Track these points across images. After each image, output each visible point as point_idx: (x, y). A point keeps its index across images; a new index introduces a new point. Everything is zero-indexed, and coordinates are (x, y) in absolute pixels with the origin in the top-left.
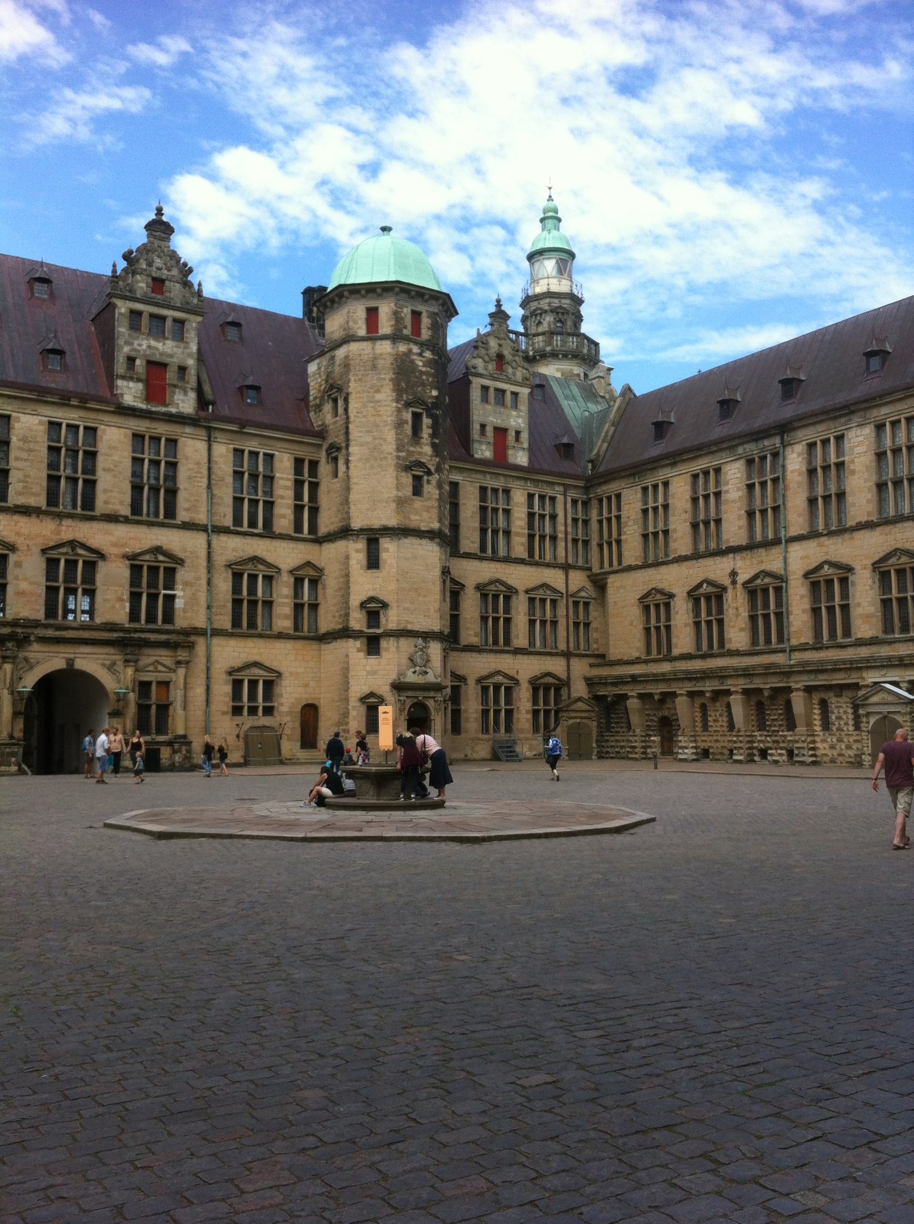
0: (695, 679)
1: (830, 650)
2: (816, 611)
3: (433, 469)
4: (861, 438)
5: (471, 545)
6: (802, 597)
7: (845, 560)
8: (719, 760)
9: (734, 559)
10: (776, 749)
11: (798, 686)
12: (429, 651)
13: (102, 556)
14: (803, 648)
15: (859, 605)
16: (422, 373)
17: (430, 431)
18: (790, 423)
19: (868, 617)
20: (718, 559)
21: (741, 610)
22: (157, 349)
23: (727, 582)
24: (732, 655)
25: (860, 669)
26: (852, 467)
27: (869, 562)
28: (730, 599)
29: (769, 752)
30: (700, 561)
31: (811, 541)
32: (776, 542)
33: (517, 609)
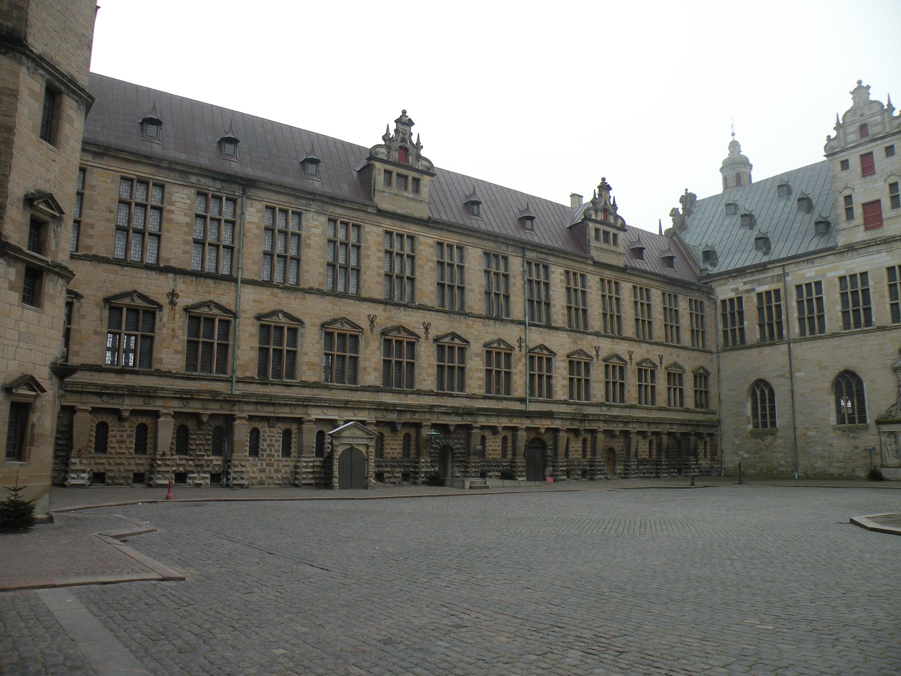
0: (108, 395)
1: (275, 387)
2: (263, 351)
4: (318, 223)
6: (251, 335)
7: (296, 314)
8: (122, 484)
9: (175, 280)
10: (198, 472)
11: (243, 415)
14: (430, 393)
15: (306, 354)
18: (260, 182)
19: (313, 364)
20: (153, 275)
21: (179, 332)
23: (164, 301)
24: (161, 376)
25: (307, 406)
26: (308, 242)
27: (318, 322)
28: (165, 319)
29: (191, 475)
30: (126, 269)
31: (265, 289)
32: (230, 279)
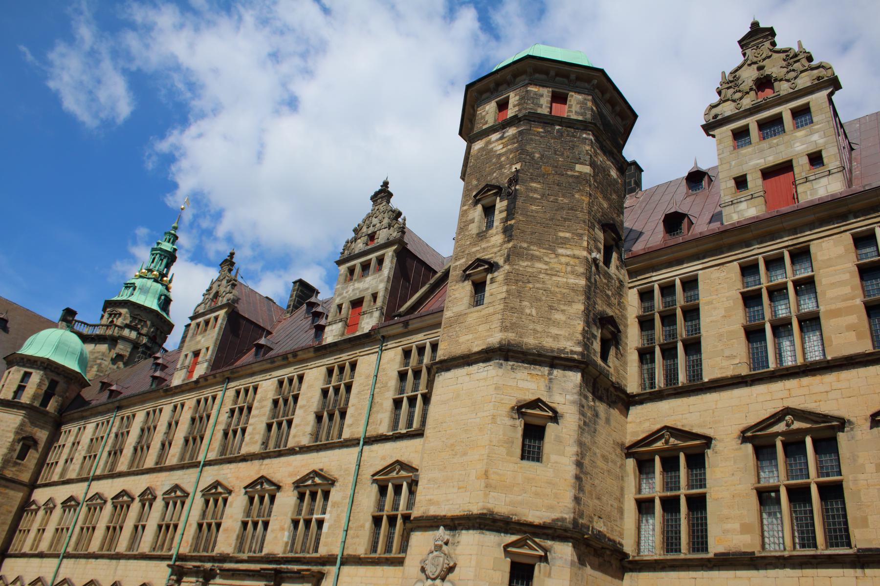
3: (501, 262)
5: (725, 363)
12: (459, 549)
13: (279, 488)
16: (500, 155)
17: (504, 214)
22: (358, 289)
33: (854, 458)
